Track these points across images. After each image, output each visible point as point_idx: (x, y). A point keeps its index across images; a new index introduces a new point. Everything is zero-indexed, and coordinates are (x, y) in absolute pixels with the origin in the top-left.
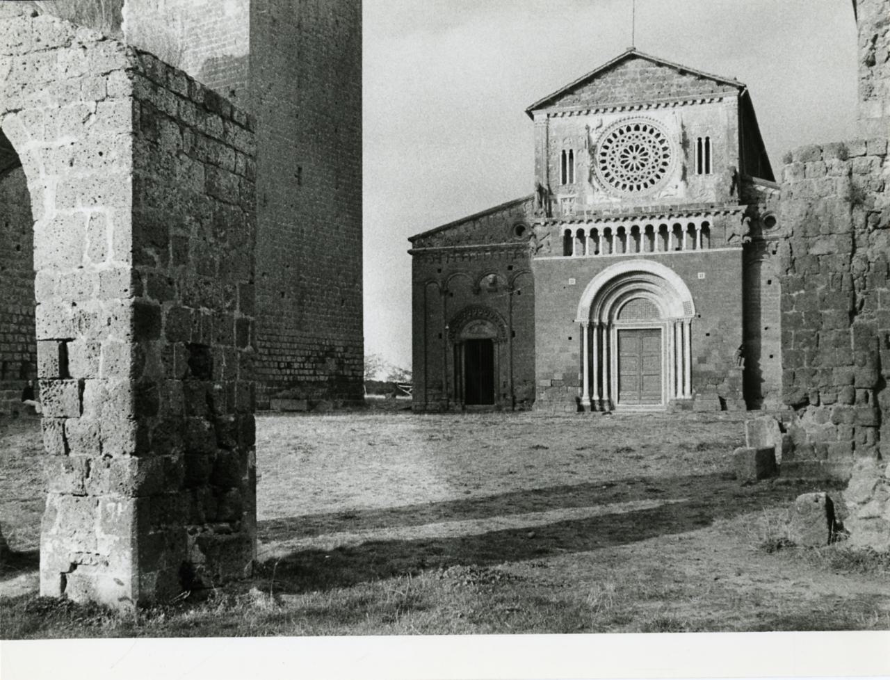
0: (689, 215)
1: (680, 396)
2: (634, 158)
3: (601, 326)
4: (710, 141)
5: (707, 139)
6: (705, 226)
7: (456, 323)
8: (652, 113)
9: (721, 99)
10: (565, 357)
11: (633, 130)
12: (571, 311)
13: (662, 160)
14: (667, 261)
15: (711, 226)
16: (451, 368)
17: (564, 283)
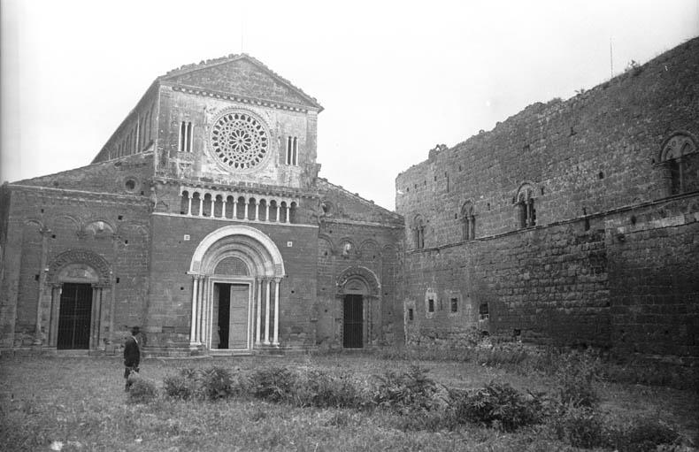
0: (284, 196)
1: (267, 342)
2: (241, 141)
5: (295, 138)
6: (293, 204)
8: (257, 110)
11: (239, 120)
13: (261, 147)
14: (266, 230)
15: (298, 205)
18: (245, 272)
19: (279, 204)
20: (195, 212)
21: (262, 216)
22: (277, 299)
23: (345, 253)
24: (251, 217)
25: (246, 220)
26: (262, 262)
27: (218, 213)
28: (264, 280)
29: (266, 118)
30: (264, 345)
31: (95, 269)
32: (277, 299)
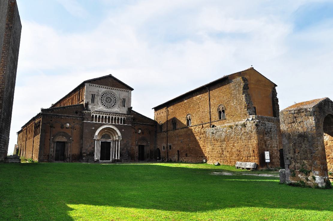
1: (116, 159)
3: (98, 140)
4: (125, 100)
6: (124, 118)
7: (54, 136)
8: (114, 91)
9: (128, 91)
10: (90, 148)
12: (93, 136)
16: (52, 150)
17: (91, 128)
18: (110, 138)
19: (120, 118)
20: (96, 121)
21: (115, 122)
22: (119, 146)
23: (139, 133)
24: (112, 122)
25: (110, 123)
26: (115, 135)
27: (102, 121)
28: (116, 141)
29: (116, 93)
30: (115, 160)
31: (66, 137)
32: (119, 146)
